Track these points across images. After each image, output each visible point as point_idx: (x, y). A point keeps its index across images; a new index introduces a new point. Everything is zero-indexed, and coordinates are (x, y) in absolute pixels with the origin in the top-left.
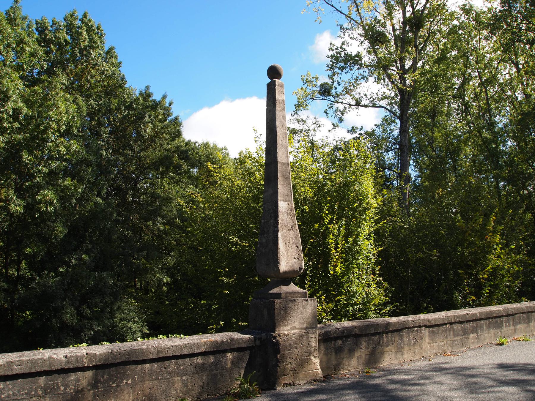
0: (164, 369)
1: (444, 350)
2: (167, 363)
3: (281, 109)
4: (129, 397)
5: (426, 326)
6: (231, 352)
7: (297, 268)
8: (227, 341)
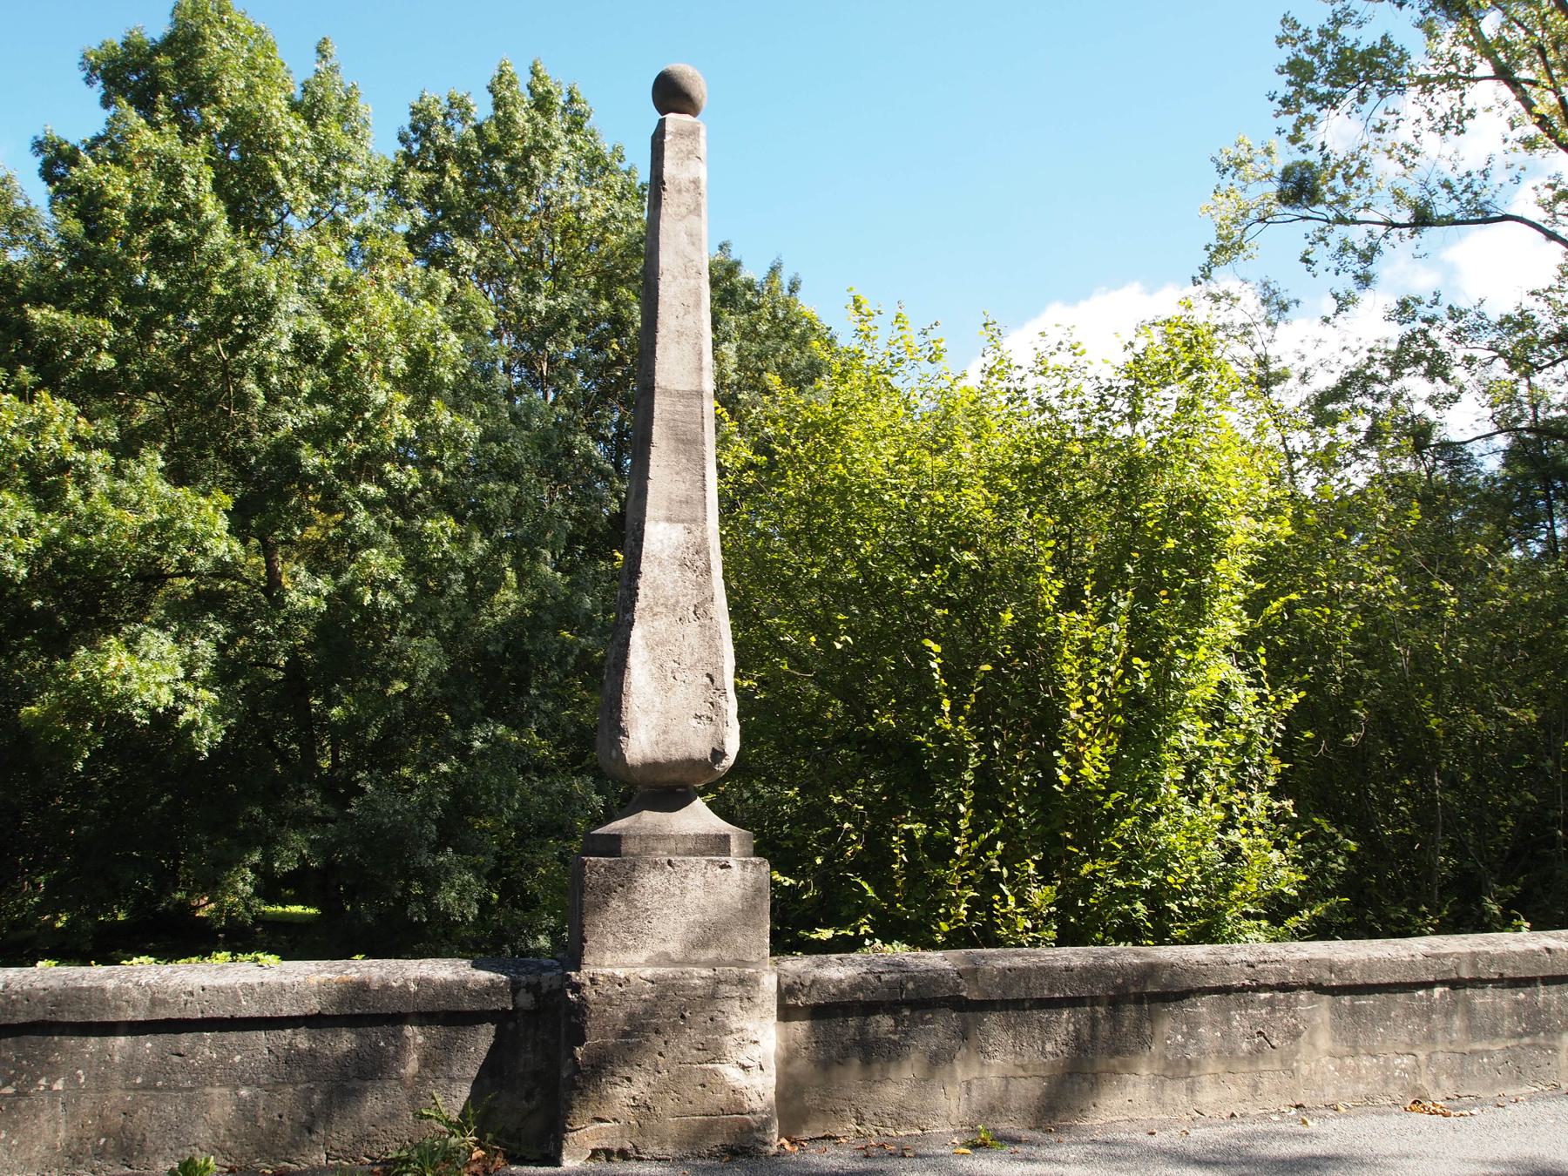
0: (176, 1059)
1: (1416, 1089)
2: (185, 1040)
3: (683, 210)
4: (56, 1131)
5: (1318, 988)
6: (421, 1025)
7: (700, 748)
8: (405, 986)
